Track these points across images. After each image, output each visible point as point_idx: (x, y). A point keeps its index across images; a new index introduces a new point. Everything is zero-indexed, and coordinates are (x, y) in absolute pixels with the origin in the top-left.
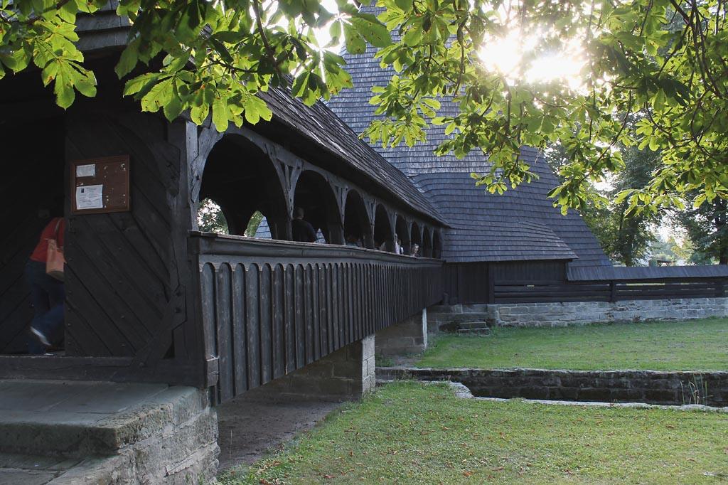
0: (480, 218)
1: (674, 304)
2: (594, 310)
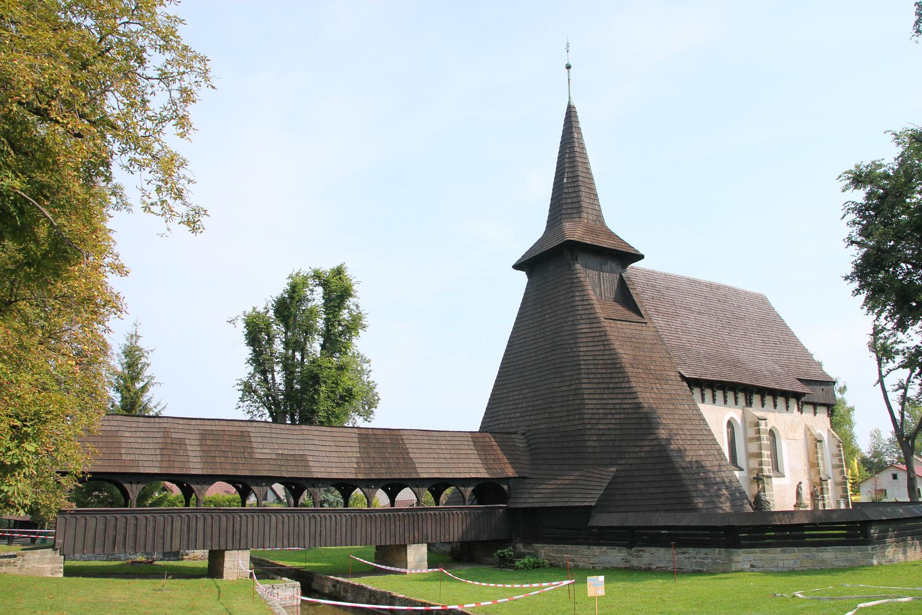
0: (555, 467)
1: (683, 553)
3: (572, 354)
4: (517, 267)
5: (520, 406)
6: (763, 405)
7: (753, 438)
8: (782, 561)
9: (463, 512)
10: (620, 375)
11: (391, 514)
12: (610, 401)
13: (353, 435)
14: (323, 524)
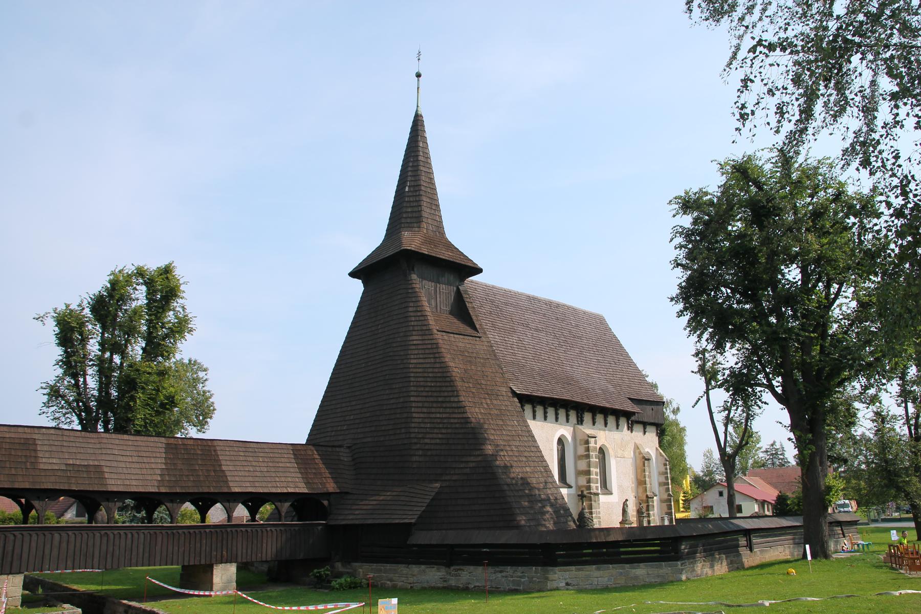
1: (501, 572)
2: (433, 575)
3: (402, 366)
4: (353, 274)
5: (347, 418)
6: (594, 424)
7: (582, 456)
8: (596, 579)
9: (278, 529)
10: (449, 389)
11: (197, 531)
12: (438, 415)
13: (160, 445)
14: (117, 542)
